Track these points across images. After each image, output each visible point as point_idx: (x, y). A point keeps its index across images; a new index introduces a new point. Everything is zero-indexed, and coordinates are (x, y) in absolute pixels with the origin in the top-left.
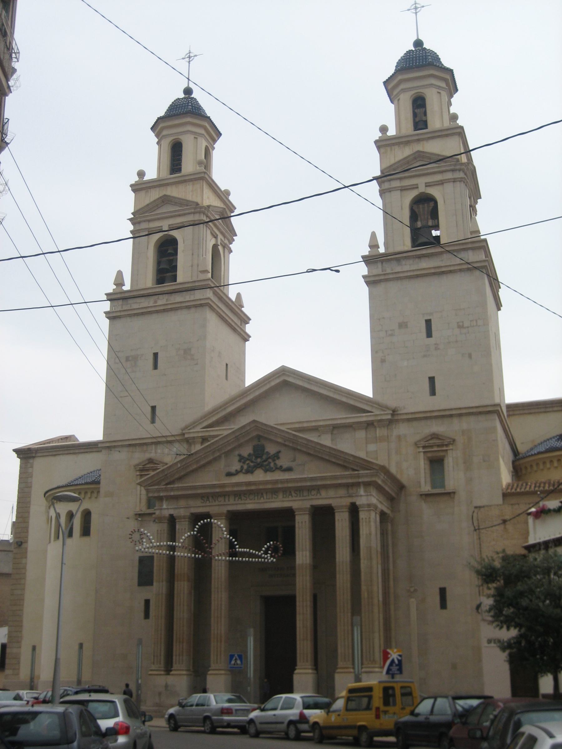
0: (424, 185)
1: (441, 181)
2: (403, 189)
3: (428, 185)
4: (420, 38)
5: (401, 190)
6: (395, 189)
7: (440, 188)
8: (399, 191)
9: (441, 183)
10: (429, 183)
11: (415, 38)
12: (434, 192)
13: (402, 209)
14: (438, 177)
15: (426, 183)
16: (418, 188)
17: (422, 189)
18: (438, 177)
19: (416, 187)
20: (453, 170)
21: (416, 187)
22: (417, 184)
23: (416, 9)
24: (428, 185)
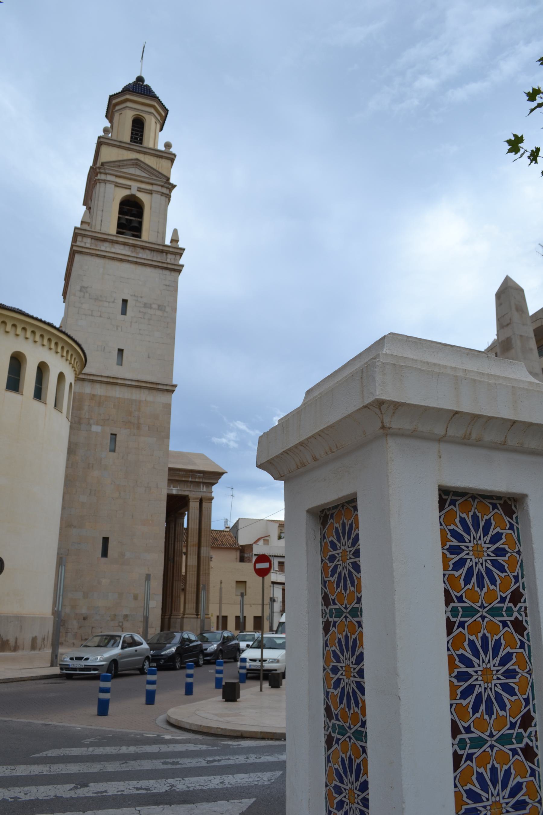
0: (136, 189)
1: (151, 191)
2: (117, 185)
5: (115, 186)
8: (114, 186)
9: (150, 192)
10: (140, 188)
12: (143, 197)
13: (113, 201)
14: (149, 187)
15: (138, 188)
16: (130, 189)
17: (134, 191)
18: (149, 187)
19: (129, 187)
20: (162, 186)
21: (129, 187)
22: (130, 186)
24: (140, 190)
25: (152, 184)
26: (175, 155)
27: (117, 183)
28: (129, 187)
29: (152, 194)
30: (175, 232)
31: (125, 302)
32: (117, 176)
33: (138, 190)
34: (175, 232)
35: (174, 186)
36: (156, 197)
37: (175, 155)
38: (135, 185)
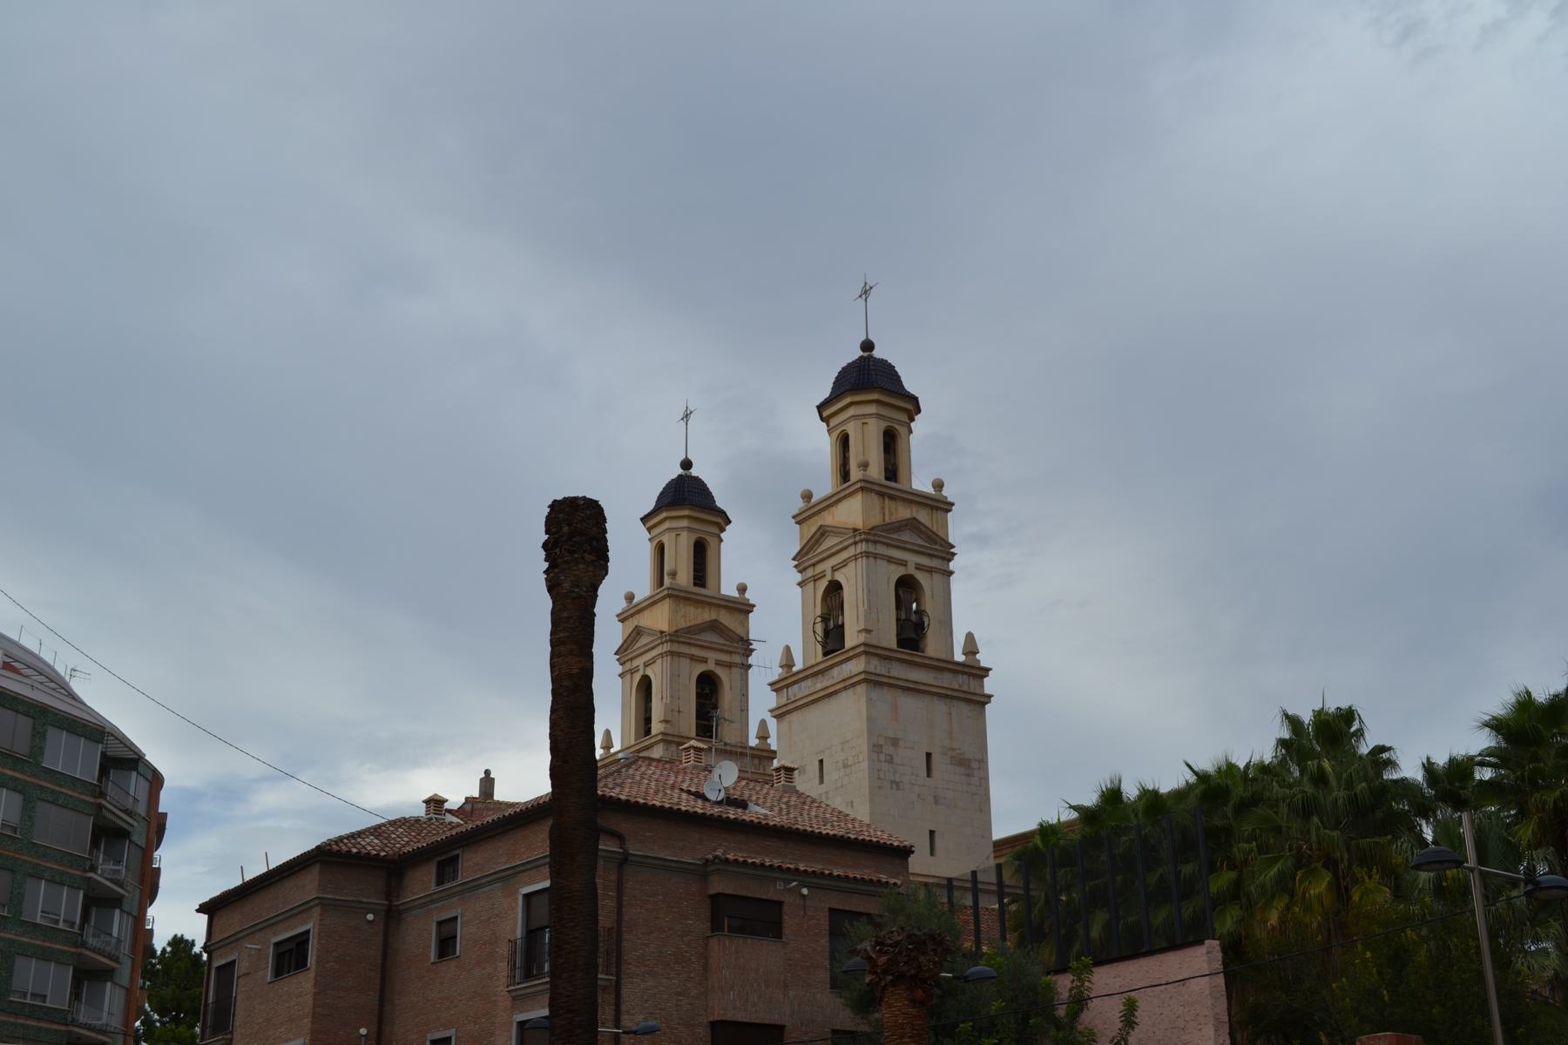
1: (931, 567)
2: (890, 560)
3: (919, 567)
4: (870, 337)
5: (888, 561)
6: (883, 557)
7: (928, 575)
9: (930, 570)
10: (919, 564)
11: (864, 338)
15: (916, 564)
17: (911, 570)
19: (903, 563)
21: (903, 563)
22: (906, 562)
23: (866, 292)
25: (931, 556)
26: (953, 504)
27: (890, 557)
28: (905, 563)
29: (932, 572)
30: (970, 638)
31: (929, 755)
32: (888, 545)
33: (916, 568)
34: (970, 638)
35: (954, 554)
36: (937, 577)
37: (953, 504)
38: (913, 559)
